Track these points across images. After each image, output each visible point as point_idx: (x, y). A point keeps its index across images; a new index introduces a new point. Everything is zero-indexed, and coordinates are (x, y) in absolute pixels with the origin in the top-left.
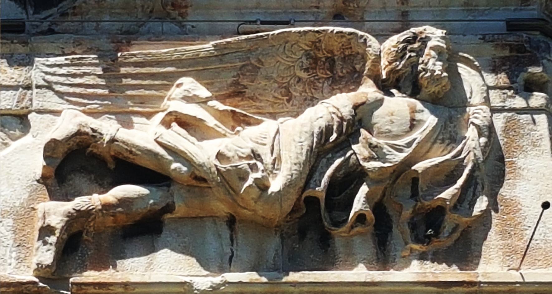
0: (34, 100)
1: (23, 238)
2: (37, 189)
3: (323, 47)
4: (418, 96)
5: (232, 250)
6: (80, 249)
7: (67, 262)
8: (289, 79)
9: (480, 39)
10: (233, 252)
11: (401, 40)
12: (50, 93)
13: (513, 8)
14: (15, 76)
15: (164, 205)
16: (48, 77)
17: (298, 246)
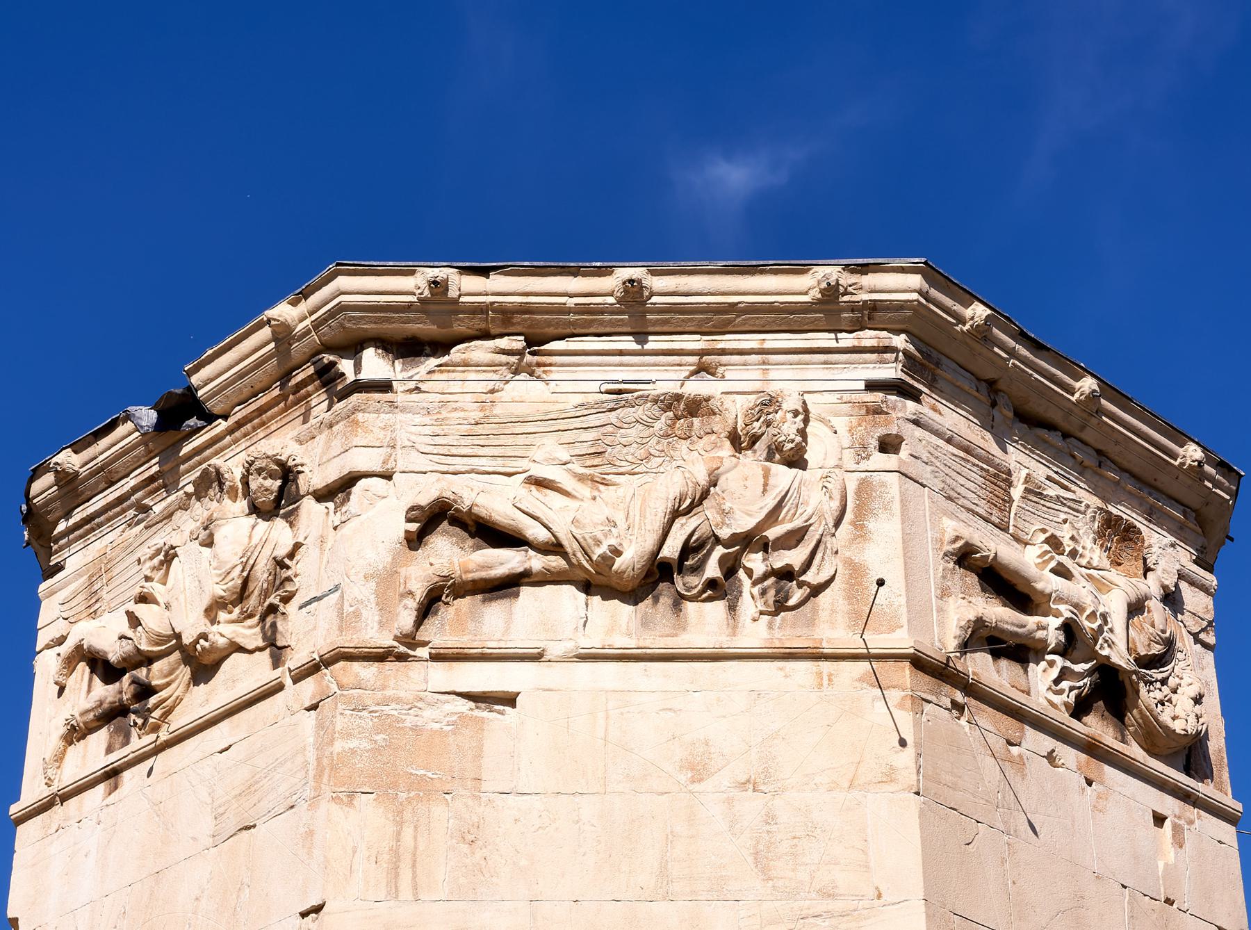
12: (414, 454)
14: (381, 436)
15: (521, 570)
16: (413, 438)
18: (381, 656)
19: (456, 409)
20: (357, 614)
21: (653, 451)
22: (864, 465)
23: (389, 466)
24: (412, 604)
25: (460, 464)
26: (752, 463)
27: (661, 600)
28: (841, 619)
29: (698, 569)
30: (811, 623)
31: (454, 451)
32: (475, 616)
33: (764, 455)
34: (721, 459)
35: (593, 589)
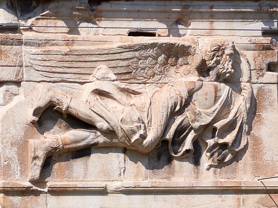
0: (24, 75)
1: (23, 159)
2: (28, 129)
3: (173, 51)
4: (219, 81)
5: (125, 166)
6: (51, 166)
7: (45, 173)
8: (154, 66)
9: (249, 41)
10: (125, 168)
11: (213, 50)
13: (265, 20)
14: (14, 60)
16: (32, 61)
17: (156, 164)
18: (24, 192)
19: (53, 44)
20: (8, 166)
21: (156, 72)
22: (260, 80)
23: (19, 78)
24: (40, 163)
25: (57, 77)
26: (209, 83)
27: (162, 158)
28: (249, 169)
29: (182, 142)
30: (234, 171)
31: (54, 70)
32: (70, 168)
33: (214, 78)
34: (194, 82)
35: (128, 152)
